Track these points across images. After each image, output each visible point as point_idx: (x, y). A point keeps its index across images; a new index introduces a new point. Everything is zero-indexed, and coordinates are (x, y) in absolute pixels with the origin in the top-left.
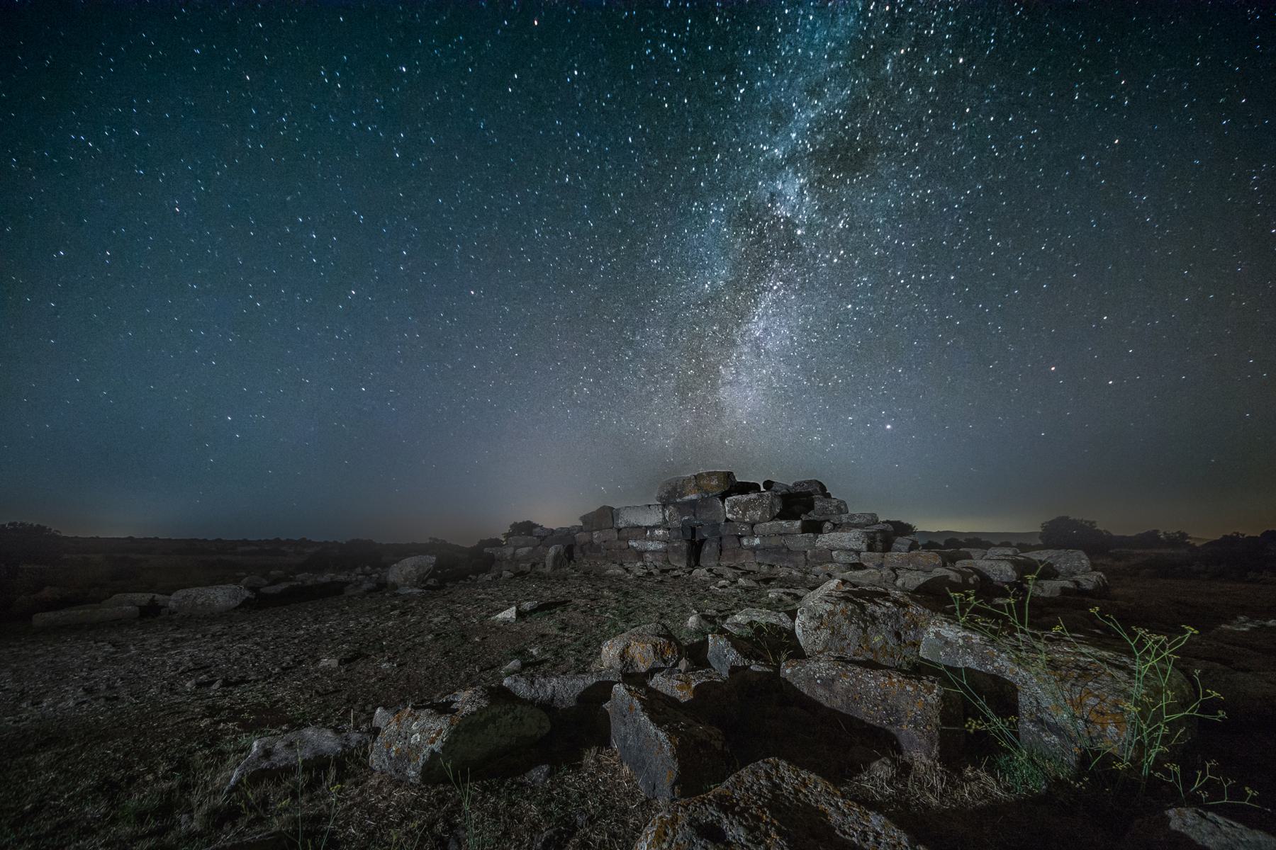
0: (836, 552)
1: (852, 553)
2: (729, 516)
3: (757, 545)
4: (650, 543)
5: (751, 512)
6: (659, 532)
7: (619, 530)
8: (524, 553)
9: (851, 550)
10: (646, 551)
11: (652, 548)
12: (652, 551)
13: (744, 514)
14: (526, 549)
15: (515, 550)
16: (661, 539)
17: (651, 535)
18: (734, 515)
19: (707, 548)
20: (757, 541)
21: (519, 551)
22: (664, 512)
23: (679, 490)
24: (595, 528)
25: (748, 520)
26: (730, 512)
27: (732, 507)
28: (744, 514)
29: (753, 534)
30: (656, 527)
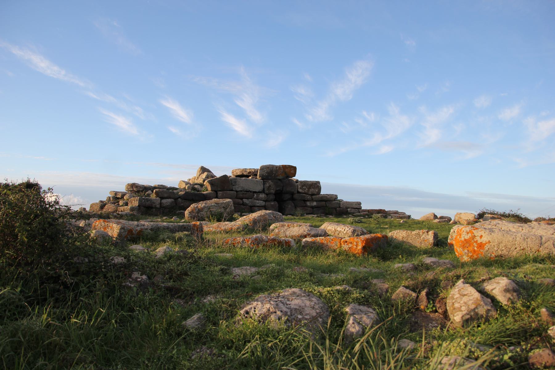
0: (350, 209)
1: (357, 209)
2: (300, 190)
3: (315, 206)
4: (257, 201)
5: (312, 190)
6: (262, 196)
7: (237, 191)
8: (168, 204)
9: (356, 208)
10: (255, 206)
11: (259, 205)
12: (258, 206)
13: (308, 191)
14: (170, 200)
15: (161, 201)
16: (262, 200)
17: (257, 197)
18: (303, 190)
19: (289, 206)
20: (315, 204)
21: (164, 201)
22: (264, 184)
23: (274, 172)
24: (219, 189)
25: (310, 193)
26: (301, 188)
27: (302, 186)
28: (308, 191)
29: (312, 200)
30: (260, 192)
